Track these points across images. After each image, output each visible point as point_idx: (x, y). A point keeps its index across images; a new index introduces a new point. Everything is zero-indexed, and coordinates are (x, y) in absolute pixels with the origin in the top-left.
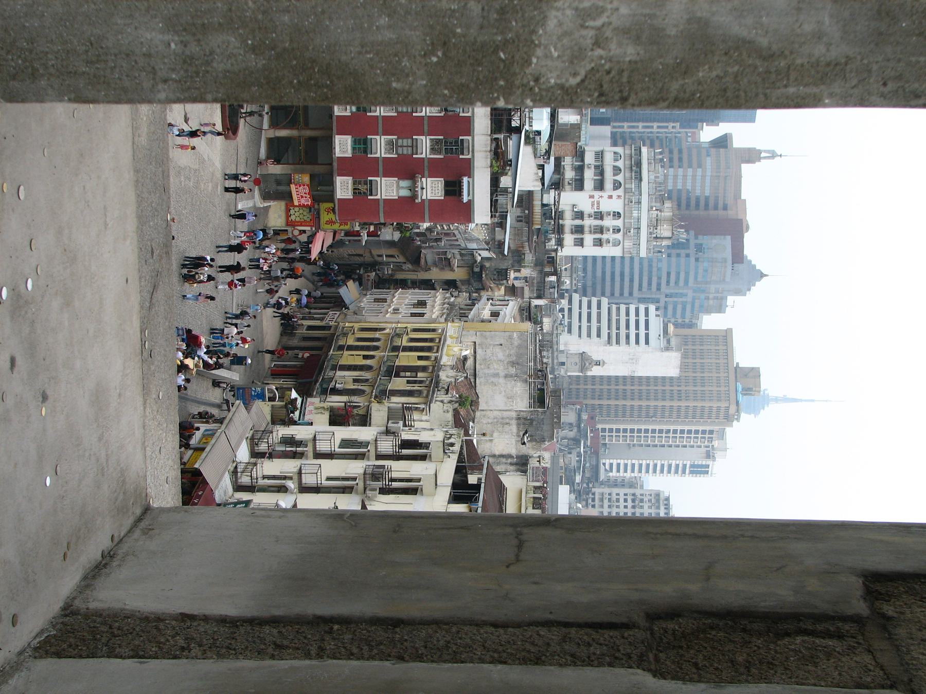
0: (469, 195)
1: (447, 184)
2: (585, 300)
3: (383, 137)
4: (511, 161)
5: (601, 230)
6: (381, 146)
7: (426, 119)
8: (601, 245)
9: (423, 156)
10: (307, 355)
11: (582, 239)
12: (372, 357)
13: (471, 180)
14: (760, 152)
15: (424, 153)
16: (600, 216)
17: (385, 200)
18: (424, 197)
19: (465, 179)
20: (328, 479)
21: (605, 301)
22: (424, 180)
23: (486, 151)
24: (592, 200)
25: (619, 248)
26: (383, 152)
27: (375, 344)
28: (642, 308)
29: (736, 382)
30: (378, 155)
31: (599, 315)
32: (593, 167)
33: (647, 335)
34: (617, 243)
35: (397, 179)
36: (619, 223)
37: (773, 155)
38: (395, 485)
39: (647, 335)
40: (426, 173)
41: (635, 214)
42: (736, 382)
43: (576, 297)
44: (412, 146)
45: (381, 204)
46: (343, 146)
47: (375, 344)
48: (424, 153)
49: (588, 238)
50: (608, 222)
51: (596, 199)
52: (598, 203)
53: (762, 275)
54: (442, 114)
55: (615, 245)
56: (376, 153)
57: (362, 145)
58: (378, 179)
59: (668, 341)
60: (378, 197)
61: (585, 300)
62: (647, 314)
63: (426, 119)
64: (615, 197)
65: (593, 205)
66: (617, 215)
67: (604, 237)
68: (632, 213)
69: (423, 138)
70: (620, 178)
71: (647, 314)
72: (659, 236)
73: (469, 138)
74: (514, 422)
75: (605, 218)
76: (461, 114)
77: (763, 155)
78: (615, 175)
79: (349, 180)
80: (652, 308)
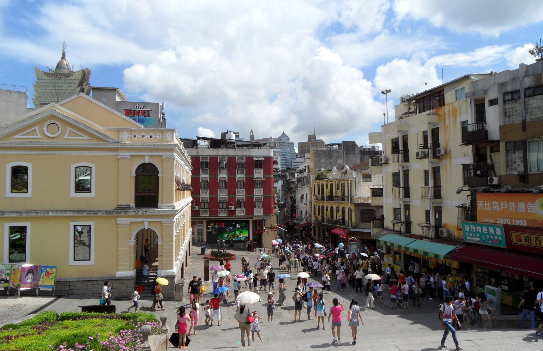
1: (257, 167)
3: (237, 195)
7: (229, 176)
9: (245, 177)
10: (327, 233)
12: (327, 207)
13: (255, 157)
14: (251, 135)
17: (264, 194)
18: (262, 177)
19: (255, 159)
20: (427, 184)
22: (255, 177)
23: (243, 151)
25: (278, 157)
26: (244, 195)
27: (321, 208)
28: (293, 164)
29: (312, 141)
30: (245, 197)
37: (252, 131)
42: (312, 141)
44: (241, 182)
46: (241, 213)
47: (321, 208)
53: (284, 133)
54: (227, 169)
55: (277, 158)
56: (244, 198)
58: (255, 197)
59: (302, 156)
60: (263, 197)
62: (295, 163)
63: (229, 176)
69: (237, 177)
71: (295, 163)
73: (237, 158)
74: (348, 156)
76: (227, 161)
77: (252, 134)
79: (255, 210)
80: (293, 161)
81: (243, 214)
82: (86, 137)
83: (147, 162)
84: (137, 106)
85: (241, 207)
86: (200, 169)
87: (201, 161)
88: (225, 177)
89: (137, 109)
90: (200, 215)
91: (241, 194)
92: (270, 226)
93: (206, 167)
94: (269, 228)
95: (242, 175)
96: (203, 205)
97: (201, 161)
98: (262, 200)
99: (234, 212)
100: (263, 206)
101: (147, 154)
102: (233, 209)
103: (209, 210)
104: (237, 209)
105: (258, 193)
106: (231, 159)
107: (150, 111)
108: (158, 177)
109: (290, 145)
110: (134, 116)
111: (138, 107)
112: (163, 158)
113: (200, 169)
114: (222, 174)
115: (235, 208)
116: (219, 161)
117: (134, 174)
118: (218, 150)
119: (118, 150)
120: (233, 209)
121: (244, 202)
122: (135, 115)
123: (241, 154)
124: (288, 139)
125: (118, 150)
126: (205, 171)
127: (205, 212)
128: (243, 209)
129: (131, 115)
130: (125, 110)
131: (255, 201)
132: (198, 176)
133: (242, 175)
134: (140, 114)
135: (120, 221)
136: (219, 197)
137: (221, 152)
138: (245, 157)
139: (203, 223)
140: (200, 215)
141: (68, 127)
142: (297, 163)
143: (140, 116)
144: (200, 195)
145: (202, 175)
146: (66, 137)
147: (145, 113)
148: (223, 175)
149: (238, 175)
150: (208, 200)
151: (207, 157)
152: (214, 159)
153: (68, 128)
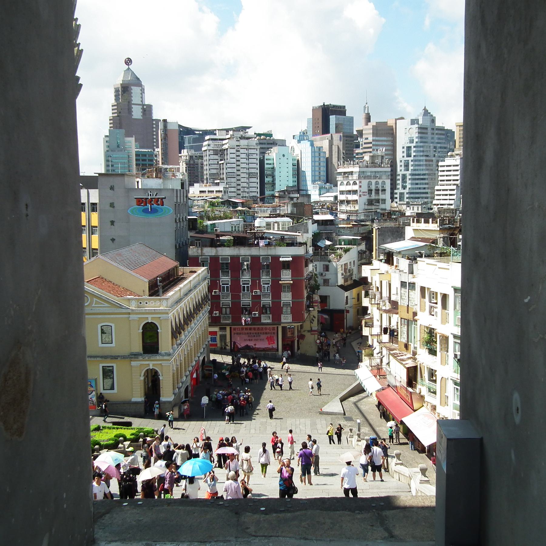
0: (289, 257)
2: (436, 197)
3: (262, 299)
4: (281, 237)
5: (377, 191)
6: (267, 300)
8: (385, 190)
11: (382, 200)
13: (281, 256)
15: (269, 279)
16: (370, 191)
18: (291, 279)
19: (281, 259)
21: (437, 188)
22: (282, 279)
23: (268, 249)
24: (362, 195)
26: (269, 299)
30: (271, 302)
31: (443, 190)
32: (347, 195)
33: (454, 166)
34: (384, 183)
35: (282, 293)
36: (373, 181)
38: (388, 295)
39: (454, 166)
40: (278, 278)
41: (369, 174)
43: (435, 202)
45: (294, 300)
48: (269, 279)
49: (381, 196)
50: (373, 187)
51: (361, 193)
52: (363, 192)
57: (263, 310)
58: (282, 302)
60: (291, 302)
61: (436, 197)
62: (444, 166)
64: (360, 184)
65: (365, 195)
66: (370, 184)
67: (380, 188)
68: (369, 176)
70: (351, 182)
71: (444, 166)
72: (381, 162)
73: (261, 257)
75: (371, 189)
78: (350, 184)
81: (269, 321)
82: (107, 305)
83: (150, 322)
84: (149, 193)
85: (266, 313)
86: (220, 271)
87: (220, 262)
88: (249, 279)
89: (149, 197)
90: (221, 322)
91: (267, 300)
92: (310, 329)
93: (226, 269)
94: (308, 331)
95: (267, 277)
96: (224, 310)
97: (220, 262)
98: (290, 305)
99: (259, 318)
100: (292, 312)
101: (150, 317)
102: (257, 315)
103: (231, 316)
104: (262, 315)
105: (285, 298)
106: (255, 259)
107: (164, 198)
108: (158, 332)
109: (437, 132)
110: (146, 205)
111: (150, 194)
112: (161, 319)
113: (220, 271)
114: (245, 276)
115: (260, 314)
116: (241, 262)
117: (141, 331)
118: (239, 249)
119: (129, 314)
120: (257, 315)
121: (270, 307)
122: (148, 204)
123: (265, 254)
124: (433, 121)
125: (129, 314)
126: (225, 273)
127: (225, 319)
128: (269, 315)
129: (143, 204)
130: (135, 198)
131: (282, 306)
132: (218, 279)
133: (267, 277)
134: (153, 202)
135: (134, 363)
136: (242, 302)
137: (243, 251)
138: (270, 257)
139: (226, 329)
140: (221, 322)
141: (94, 298)
142: (447, 166)
143: (153, 205)
144: (221, 300)
145: (222, 278)
146: (93, 305)
147: (158, 201)
148: (246, 278)
149: (263, 277)
150: (229, 305)
151: (227, 257)
152: (235, 259)
153: (95, 299)
